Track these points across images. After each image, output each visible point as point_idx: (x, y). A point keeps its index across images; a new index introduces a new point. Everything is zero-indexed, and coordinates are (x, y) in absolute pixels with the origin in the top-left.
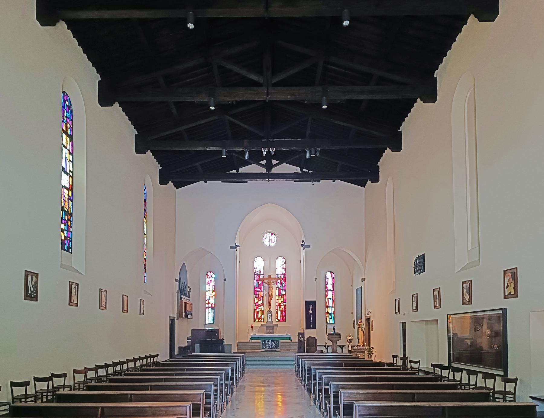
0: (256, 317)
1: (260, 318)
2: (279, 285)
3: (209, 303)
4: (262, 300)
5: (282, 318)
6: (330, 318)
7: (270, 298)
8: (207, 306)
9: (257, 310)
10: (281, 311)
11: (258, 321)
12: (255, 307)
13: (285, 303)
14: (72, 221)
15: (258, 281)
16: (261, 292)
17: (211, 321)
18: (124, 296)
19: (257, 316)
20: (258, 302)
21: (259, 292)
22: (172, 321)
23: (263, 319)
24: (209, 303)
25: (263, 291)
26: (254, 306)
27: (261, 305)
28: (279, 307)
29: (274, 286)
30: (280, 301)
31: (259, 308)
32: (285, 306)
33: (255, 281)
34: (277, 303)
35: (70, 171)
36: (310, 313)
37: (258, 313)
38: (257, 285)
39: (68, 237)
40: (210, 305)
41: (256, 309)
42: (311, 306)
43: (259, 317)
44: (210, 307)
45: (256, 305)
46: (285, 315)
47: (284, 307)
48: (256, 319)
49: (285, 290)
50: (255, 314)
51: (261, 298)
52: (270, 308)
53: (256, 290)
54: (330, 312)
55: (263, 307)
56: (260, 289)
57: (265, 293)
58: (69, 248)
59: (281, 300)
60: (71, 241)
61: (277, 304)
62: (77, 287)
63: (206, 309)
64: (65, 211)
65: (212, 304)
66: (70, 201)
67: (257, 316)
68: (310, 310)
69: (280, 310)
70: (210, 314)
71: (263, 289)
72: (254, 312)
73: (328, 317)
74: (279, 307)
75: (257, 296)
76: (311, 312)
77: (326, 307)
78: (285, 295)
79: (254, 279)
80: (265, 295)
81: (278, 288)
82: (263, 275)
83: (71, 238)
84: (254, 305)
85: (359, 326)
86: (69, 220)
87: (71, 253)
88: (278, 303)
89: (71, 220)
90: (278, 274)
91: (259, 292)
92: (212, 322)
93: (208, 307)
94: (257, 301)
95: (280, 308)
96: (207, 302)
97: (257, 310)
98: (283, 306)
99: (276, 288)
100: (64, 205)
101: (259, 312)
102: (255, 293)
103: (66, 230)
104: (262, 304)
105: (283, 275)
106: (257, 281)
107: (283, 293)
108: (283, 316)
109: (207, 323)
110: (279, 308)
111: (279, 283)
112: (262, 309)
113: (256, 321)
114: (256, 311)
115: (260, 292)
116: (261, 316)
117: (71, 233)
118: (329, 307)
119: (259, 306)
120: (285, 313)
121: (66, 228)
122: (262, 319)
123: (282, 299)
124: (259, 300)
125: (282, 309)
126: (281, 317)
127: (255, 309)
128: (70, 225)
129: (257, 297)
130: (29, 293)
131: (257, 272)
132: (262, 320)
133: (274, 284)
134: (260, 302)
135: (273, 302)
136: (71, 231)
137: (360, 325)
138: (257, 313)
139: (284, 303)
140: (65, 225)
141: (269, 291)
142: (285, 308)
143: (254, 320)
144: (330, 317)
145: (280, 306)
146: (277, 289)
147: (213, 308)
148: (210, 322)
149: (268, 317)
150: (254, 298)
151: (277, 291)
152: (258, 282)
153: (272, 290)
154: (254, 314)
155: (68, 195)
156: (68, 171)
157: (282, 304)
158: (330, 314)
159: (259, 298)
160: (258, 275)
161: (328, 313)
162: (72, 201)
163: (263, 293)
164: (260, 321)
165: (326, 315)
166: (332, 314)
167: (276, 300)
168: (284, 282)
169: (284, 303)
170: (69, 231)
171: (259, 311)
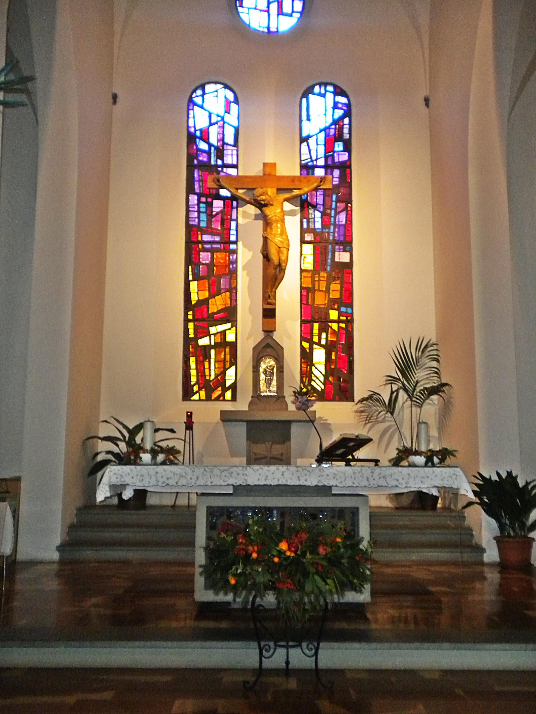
0: (194, 380)
10: (329, 348)
11: (208, 398)
12: (191, 325)
15: (207, 197)
21: (212, 251)
23: (234, 387)
25: (232, 247)
26: (186, 321)
28: (316, 326)
30: (320, 300)
31: (213, 330)
33: (194, 199)
38: (203, 217)
43: (212, 374)
48: (196, 388)
50: (193, 360)
52: (269, 332)
56: (217, 239)
71: (233, 238)
74: (316, 326)
79: (190, 190)
80: (244, 268)
81: (313, 231)
82: (232, 172)
84: (186, 315)
95: (324, 335)
97: (203, 342)
99: (303, 232)
101: (213, 352)
105: (336, 173)
106: (203, 199)
107: (337, 260)
110: (321, 330)
112: (230, 337)
113: (196, 397)
116: (223, 374)
122: (228, 384)
123: (335, 286)
127: (192, 335)
129: (203, 278)
131: (203, 158)
132: (228, 395)
133: (292, 213)
138: (204, 352)
139: (343, 309)
141: (265, 239)
143: (187, 393)
146: (308, 237)
149: (262, 377)
151: (309, 249)
152: (209, 205)
153: (283, 232)
157: (334, 315)
160: (206, 167)
168: (341, 205)
171: (209, 347)
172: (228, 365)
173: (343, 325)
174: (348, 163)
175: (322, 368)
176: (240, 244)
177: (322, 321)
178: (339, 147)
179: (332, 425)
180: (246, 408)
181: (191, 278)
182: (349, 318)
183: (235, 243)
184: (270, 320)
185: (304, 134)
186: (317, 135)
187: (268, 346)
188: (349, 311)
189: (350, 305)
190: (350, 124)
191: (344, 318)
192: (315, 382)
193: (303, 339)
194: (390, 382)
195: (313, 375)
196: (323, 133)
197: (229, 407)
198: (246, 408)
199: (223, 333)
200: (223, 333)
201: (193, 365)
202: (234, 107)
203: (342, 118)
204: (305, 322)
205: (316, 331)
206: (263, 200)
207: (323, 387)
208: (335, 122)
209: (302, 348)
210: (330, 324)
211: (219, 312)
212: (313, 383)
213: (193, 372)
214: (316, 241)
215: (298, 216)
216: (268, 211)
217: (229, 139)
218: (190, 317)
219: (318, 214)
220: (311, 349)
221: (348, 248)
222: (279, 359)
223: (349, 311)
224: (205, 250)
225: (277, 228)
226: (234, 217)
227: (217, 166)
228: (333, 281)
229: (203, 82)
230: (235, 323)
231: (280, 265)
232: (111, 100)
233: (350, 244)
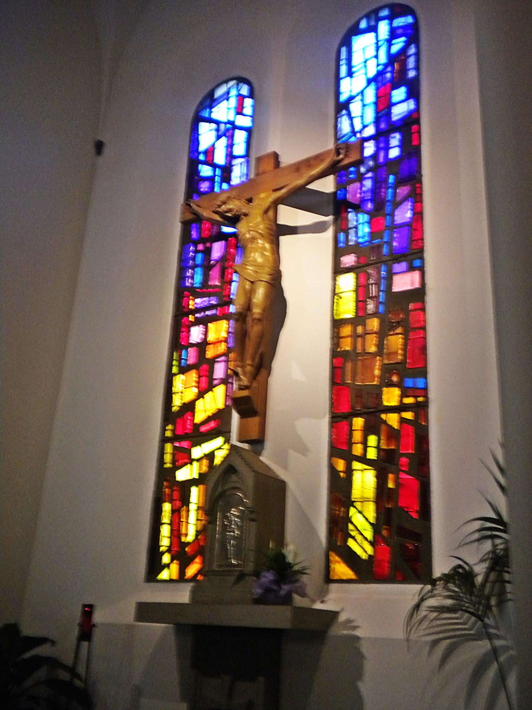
0: (165, 542)
12: (169, 448)
31: (197, 452)
37: (185, 501)
48: (166, 559)
49: (420, 253)
50: (167, 507)
74: (358, 422)
91: (204, 322)
94: (191, 393)
95: (372, 440)
105: (395, 140)
110: (367, 431)
113: (164, 575)
146: (349, 260)
173: (408, 415)
174: (415, 115)
175: (371, 511)
177: (371, 412)
178: (399, 94)
179: (363, 642)
181: (175, 370)
182: (420, 399)
185: (343, 98)
186: (362, 92)
188: (420, 383)
189: (423, 373)
190: (417, 55)
191: (409, 400)
192: (356, 540)
194: (489, 533)
195: (351, 527)
196: (373, 87)
199: (210, 456)
201: (166, 518)
202: (248, 103)
203: (403, 51)
204: (339, 419)
205: (357, 436)
206: (230, 211)
207: (370, 550)
208: (392, 59)
209: (333, 471)
210: (383, 416)
211: (209, 419)
212: (351, 543)
213: (165, 531)
214: (360, 265)
217: (239, 149)
218: (168, 434)
219: (363, 218)
220: (349, 471)
221: (417, 263)
228: (390, 330)
229: (209, 88)
230: (229, 434)
232: (93, 150)
233: (419, 255)
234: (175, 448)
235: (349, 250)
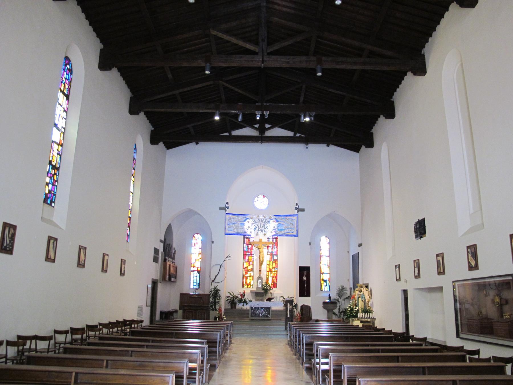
0: (244, 283)
1: (250, 284)
2: (270, 249)
3: (194, 267)
4: (252, 265)
5: (273, 285)
6: (325, 286)
7: (261, 263)
8: (192, 269)
9: (246, 276)
10: (273, 277)
11: (248, 287)
12: (244, 272)
13: (277, 268)
14: (58, 175)
15: (248, 244)
16: (251, 256)
17: (196, 285)
18: (104, 255)
19: (246, 282)
20: (247, 267)
22: (155, 283)
23: (253, 285)
24: (194, 267)
25: (253, 255)
26: (243, 271)
27: (250, 270)
29: (265, 251)
30: (271, 267)
31: (249, 273)
32: (277, 272)
33: (245, 245)
34: (268, 269)
35: (62, 127)
36: (304, 280)
39: (52, 191)
40: (195, 269)
41: (245, 275)
42: (305, 272)
44: (195, 271)
45: (246, 270)
46: (277, 281)
47: (276, 273)
48: (245, 285)
49: (277, 255)
50: (244, 279)
51: (251, 263)
52: (260, 274)
53: (246, 254)
54: (325, 279)
55: (253, 272)
56: (250, 254)
57: (255, 258)
58: (52, 202)
59: (272, 265)
60: (55, 195)
61: (268, 270)
62: (55, 242)
63: (192, 272)
64: (52, 165)
65: (198, 268)
66: (59, 156)
67: (246, 282)
68: (304, 277)
69: (271, 276)
70: (195, 278)
71: (253, 254)
72: (243, 277)
73: (322, 284)
75: (246, 260)
76: (305, 278)
77: (321, 273)
78: (277, 260)
79: (244, 243)
81: (270, 252)
83: (56, 192)
85: (359, 296)
86: (55, 174)
87: (54, 207)
88: (269, 269)
89: (58, 174)
90: (270, 238)
91: (249, 256)
92: (197, 287)
93: (194, 271)
94: (247, 266)
96: (192, 265)
97: (246, 276)
98: (274, 272)
99: (267, 252)
100: (53, 159)
101: (248, 278)
102: (244, 258)
103: (51, 184)
104: (252, 270)
105: (275, 239)
106: (247, 245)
107: (274, 258)
108: (274, 282)
109: (192, 287)
110: (271, 273)
111: (270, 247)
112: (252, 275)
114: (245, 277)
115: (250, 256)
117: (56, 187)
118: (323, 273)
119: (248, 271)
120: (277, 280)
121: (51, 182)
123: (274, 264)
124: (249, 264)
125: (273, 275)
126: (273, 284)
127: (244, 274)
128: (55, 179)
130: (4, 246)
132: (252, 287)
133: (265, 248)
134: (250, 268)
135: (264, 267)
136: (56, 184)
137: (360, 295)
138: (246, 278)
139: (275, 269)
140: (51, 178)
141: (260, 256)
142: (277, 275)
143: (243, 286)
144: (325, 284)
145: (271, 272)
147: (199, 272)
148: (195, 287)
149: (259, 284)
150: (243, 263)
152: (248, 246)
154: (243, 280)
155: (58, 150)
156: (60, 128)
157: (273, 270)
158: (325, 281)
159: (249, 262)
160: (247, 238)
161: (323, 280)
162: (60, 156)
163: (253, 258)
164: (249, 287)
165: (321, 282)
166: (327, 281)
167: (268, 265)
168: (276, 247)
169: (276, 268)
170: (54, 185)
171: (248, 277)
172: (252, 280)
176: (254, 255)
180: (255, 290)
181: (244, 262)
183: (253, 254)
184: (260, 272)
187: (260, 277)
193: (267, 275)
197: (252, 290)
198: (255, 290)
200: (251, 274)
215: (267, 249)
216: (260, 250)
222: (262, 280)
223: (277, 269)
224: (247, 256)
225: (262, 253)
226: (253, 249)
227: (250, 238)
231: (262, 261)
234: (245, 272)
235: (269, 252)
